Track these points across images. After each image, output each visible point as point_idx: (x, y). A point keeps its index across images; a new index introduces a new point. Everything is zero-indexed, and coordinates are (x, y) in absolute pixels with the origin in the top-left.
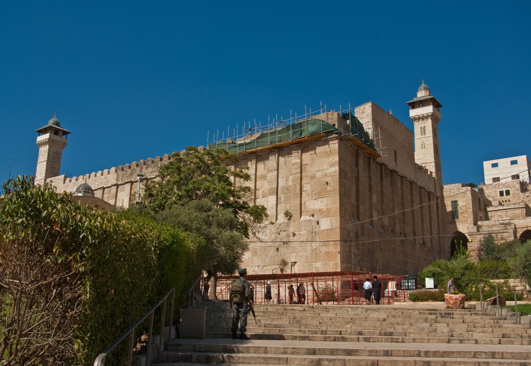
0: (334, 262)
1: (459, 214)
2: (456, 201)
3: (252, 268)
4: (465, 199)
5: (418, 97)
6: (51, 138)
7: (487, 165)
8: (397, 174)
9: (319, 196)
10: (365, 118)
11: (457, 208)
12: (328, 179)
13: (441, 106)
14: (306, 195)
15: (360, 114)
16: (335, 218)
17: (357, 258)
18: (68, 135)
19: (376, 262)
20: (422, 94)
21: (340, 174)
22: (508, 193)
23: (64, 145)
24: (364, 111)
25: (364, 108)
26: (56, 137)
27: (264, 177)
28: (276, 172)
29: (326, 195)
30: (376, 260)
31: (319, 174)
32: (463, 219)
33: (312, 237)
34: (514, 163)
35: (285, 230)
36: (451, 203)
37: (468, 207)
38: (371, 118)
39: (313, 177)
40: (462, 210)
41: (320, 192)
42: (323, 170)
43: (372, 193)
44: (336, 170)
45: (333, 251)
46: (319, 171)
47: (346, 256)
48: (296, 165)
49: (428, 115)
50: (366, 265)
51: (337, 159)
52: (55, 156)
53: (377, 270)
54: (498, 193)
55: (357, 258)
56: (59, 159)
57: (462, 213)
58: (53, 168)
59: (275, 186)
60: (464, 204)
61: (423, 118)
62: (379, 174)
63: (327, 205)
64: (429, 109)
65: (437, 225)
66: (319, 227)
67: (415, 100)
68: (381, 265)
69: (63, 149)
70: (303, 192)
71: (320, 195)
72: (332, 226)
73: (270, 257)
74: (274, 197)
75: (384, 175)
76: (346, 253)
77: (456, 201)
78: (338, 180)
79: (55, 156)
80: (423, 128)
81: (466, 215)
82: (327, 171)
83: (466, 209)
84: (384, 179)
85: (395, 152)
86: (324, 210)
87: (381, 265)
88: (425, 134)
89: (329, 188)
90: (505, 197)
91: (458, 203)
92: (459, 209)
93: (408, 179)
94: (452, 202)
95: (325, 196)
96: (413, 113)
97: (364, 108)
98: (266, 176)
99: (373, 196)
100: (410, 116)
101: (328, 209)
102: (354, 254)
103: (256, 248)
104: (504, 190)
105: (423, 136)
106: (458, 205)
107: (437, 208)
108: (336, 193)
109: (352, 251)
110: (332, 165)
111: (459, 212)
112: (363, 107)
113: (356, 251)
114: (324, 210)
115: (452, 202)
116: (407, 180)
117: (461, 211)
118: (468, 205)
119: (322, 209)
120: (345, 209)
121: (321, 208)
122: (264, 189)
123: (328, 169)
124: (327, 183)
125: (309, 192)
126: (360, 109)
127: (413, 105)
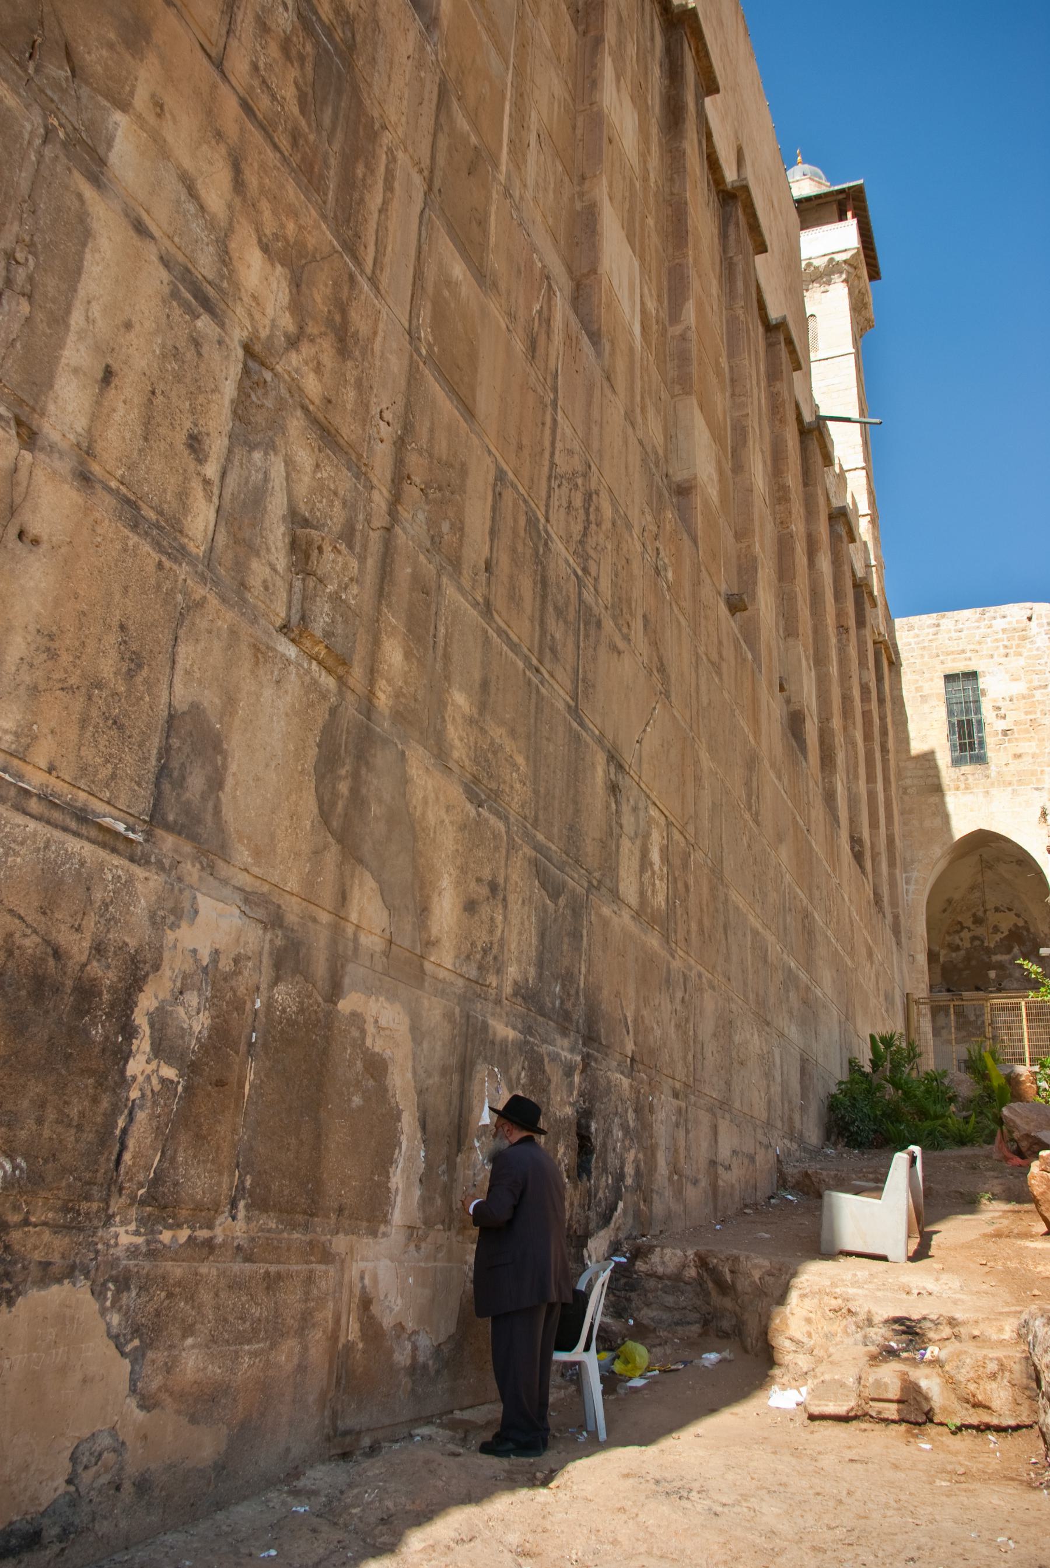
1: (990, 741)
2: (972, 675)
4: (1022, 661)
11: (978, 711)
19: (614, 789)
30: (614, 758)
32: (1015, 766)
36: (942, 683)
37: (1043, 702)
40: (1004, 717)
43: (599, 40)
49: (832, 259)
53: (615, 896)
57: (1005, 732)
68: (655, 856)
81: (1028, 747)
83: (1027, 713)
87: (655, 856)
91: (983, 683)
92: (987, 713)
94: (950, 678)
106: (984, 693)
111: (987, 729)
117: (1001, 725)
118: (1038, 695)
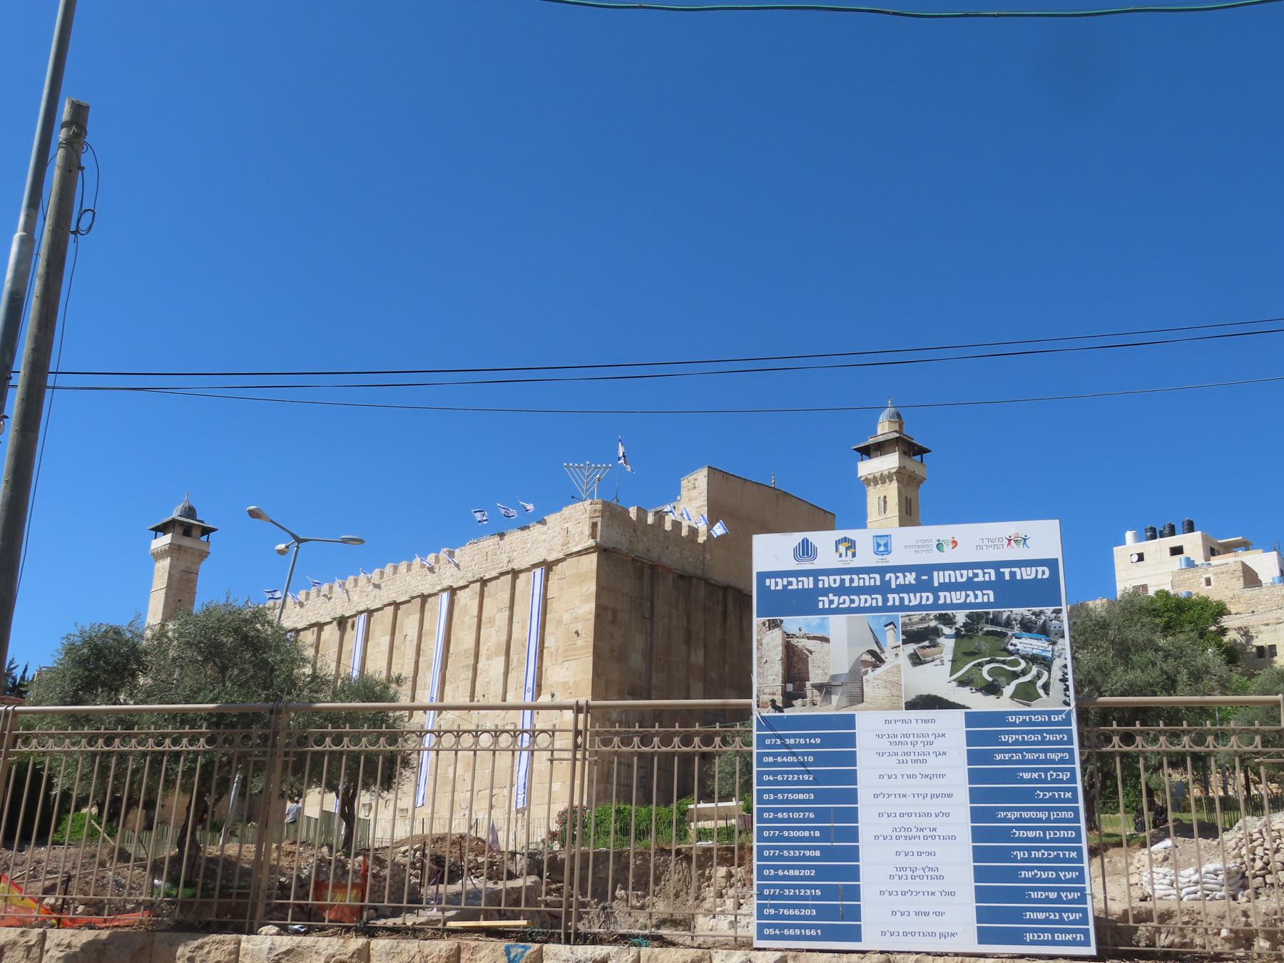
3: (462, 795)
5: (879, 432)
6: (174, 542)
9: (564, 657)
10: (696, 498)
12: (579, 627)
13: (927, 451)
20: (884, 428)
21: (598, 615)
23: (204, 555)
25: (695, 480)
26: (186, 542)
27: (492, 620)
28: (507, 613)
31: (566, 617)
38: (706, 498)
39: (559, 622)
41: (567, 651)
42: (573, 609)
46: (567, 611)
51: (592, 587)
56: (192, 584)
58: (180, 601)
59: (504, 638)
61: (883, 479)
64: (890, 462)
66: (562, 717)
67: (871, 441)
69: (200, 562)
70: (545, 651)
74: (502, 659)
75: (730, 608)
78: (592, 628)
82: (579, 612)
89: (580, 642)
95: (570, 658)
96: (868, 468)
97: (695, 480)
98: (494, 620)
99: (692, 652)
100: (859, 476)
105: (883, 516)
108: (589, 653)
110: (586, 600)
112: (695, 476)
119: (568, 682)
121: (567, 680)
122: (489, 644)
123: (579, 608)
124: (577, 633)
125: (553, 649)
127: (867, 452)
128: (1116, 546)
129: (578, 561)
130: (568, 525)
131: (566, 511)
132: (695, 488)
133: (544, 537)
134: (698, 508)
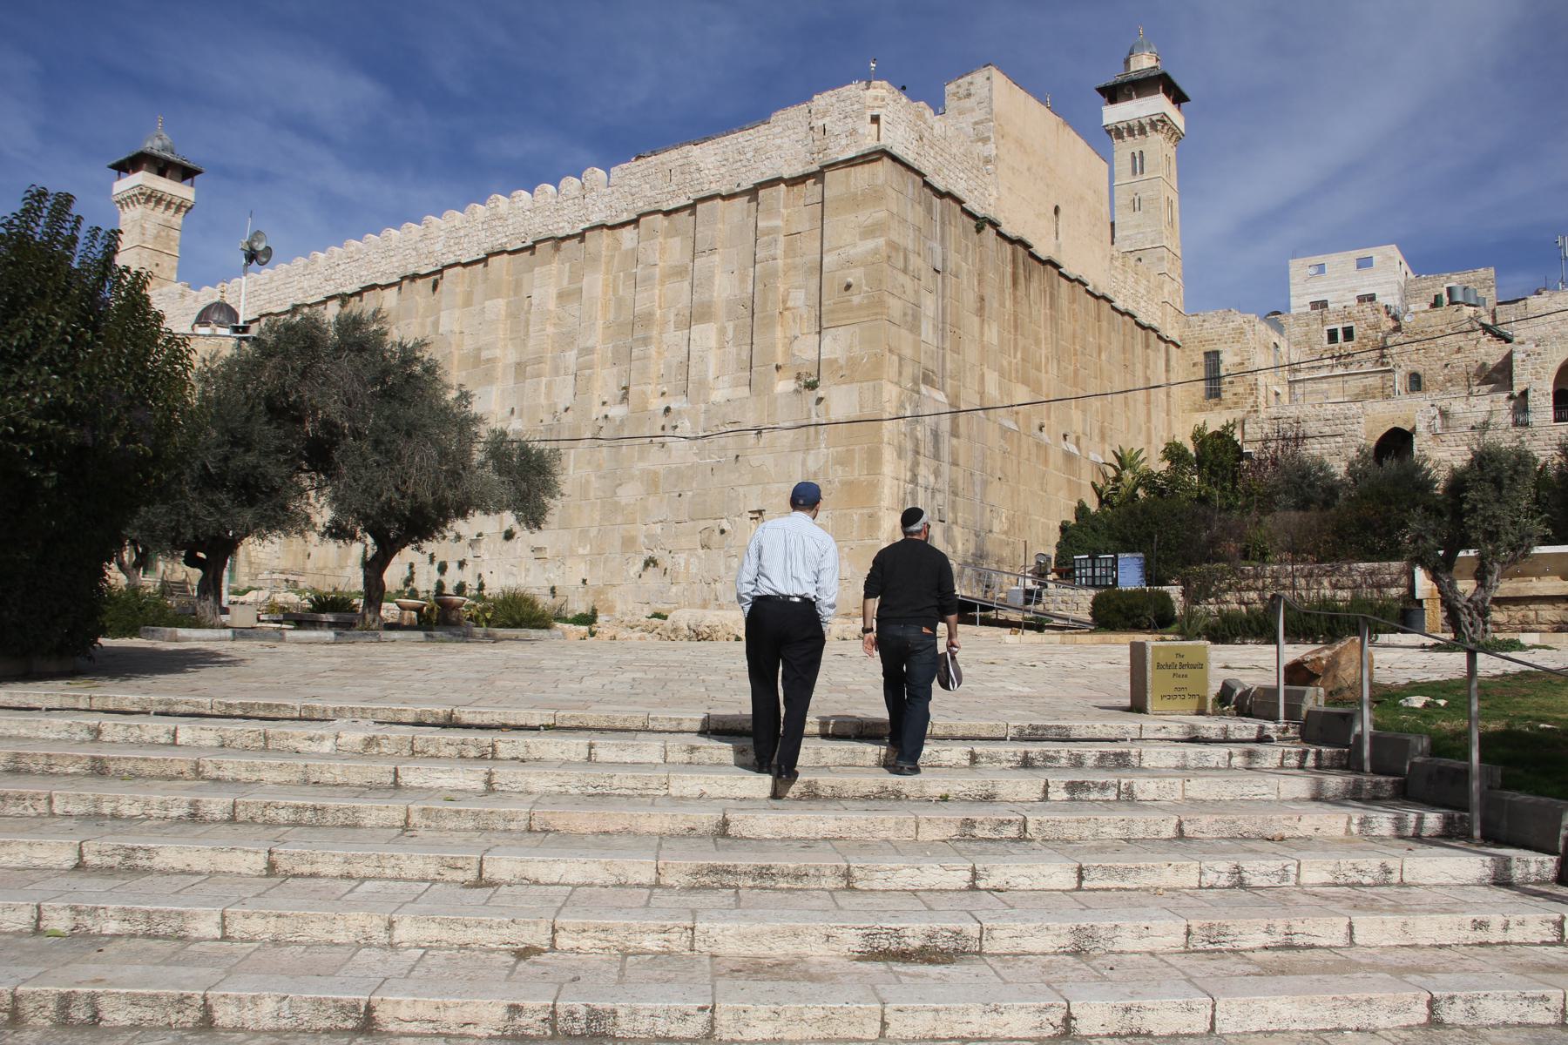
0: (865, 511)
2: (1217, 353)
7: (1299, 269)
8: (1061, 274)
10: (973, 110)
14: (794, 321)
15: (960, 99)
16: (871, 383)
17: (933, 497)
18: (196, 177)
22: (1348, 334)
24: (973, 91)
25: (971, 83)
29: (848, 318)
33: (808, 438)
34: (1364, 263)
35: (735, 419)
44: (876, 251)
45: (862, 478)
47: (901, 493)
48: (768, 234)
50: (959, 521)
52: (163, 234)
54: (1326, 336)
55: (933, 497)
60: (1237, 359)
62: (1009, 269)
63: (851, 347)
65: (1164, 415)
71: (832, 320)
72: (861, 407)
73: (693, 496)
75: (1021, 271)
76: (902, 483)
77: (1217, 353)
79: (163, 234)
80: (1137, 155)
84: (1022, 280)
85: (1057, 210)
86: (842, 362)
88: (1142, 172)
89: (856, 300)
90: (1342, 345)
91: (1222, 357)
93: (1090, 288)
94: (1207, 354)
97: (971, 83)
99: (986, 326)
101: (852, 358)
102: (926, 488)
103: (655, 473)
104: (1339, 327)
107: (1167, 371)
109: (921, 480)
113: (932, 479)
114: (842, 362)
115: (1207, 354)
116: (1087, 291)
119: (836, 360)
120: (901, 359)
121: (833, 356)
122: (679, 306)
126: (959, 87)
127: (1113, 94)
128: (1294, 256)
129: (848, 176)
130: (826, 120)
131: (820, 101)
132: (969, 95)
133: (778, 141)
134: (976, 123)
